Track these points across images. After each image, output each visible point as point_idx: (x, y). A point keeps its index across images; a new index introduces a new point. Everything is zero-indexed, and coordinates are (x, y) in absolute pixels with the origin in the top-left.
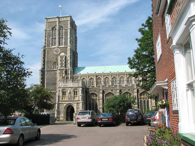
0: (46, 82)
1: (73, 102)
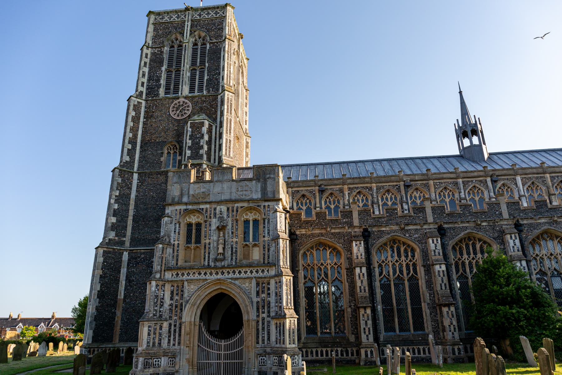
0: (131, 213)
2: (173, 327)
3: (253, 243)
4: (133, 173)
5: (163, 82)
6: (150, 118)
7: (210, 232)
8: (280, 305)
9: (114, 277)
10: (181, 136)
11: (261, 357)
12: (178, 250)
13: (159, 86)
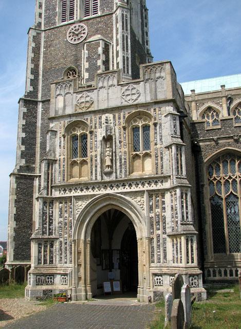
1: (127, 189)
2: (63, 244)
3: (144, 152)
6: (49, 47)
7: (96, 143)
8: (177, 220)
9: (27, 201)
11: (157, 277)
12: (64, 165)
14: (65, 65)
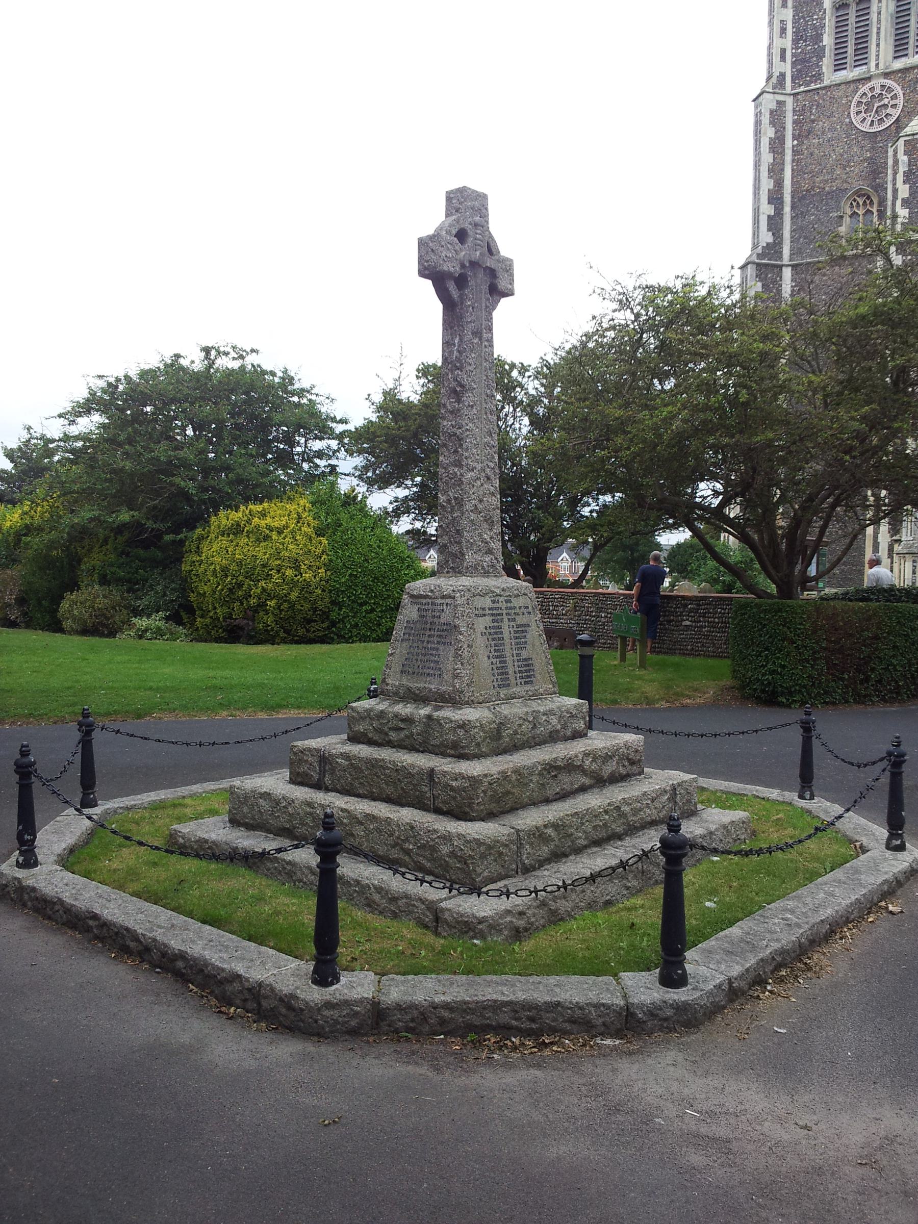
4: (781, 267)
5: (828, 40)
6: (807, 137)
10: (882, 173)
13: (821, 56)
14: (846, 182)
